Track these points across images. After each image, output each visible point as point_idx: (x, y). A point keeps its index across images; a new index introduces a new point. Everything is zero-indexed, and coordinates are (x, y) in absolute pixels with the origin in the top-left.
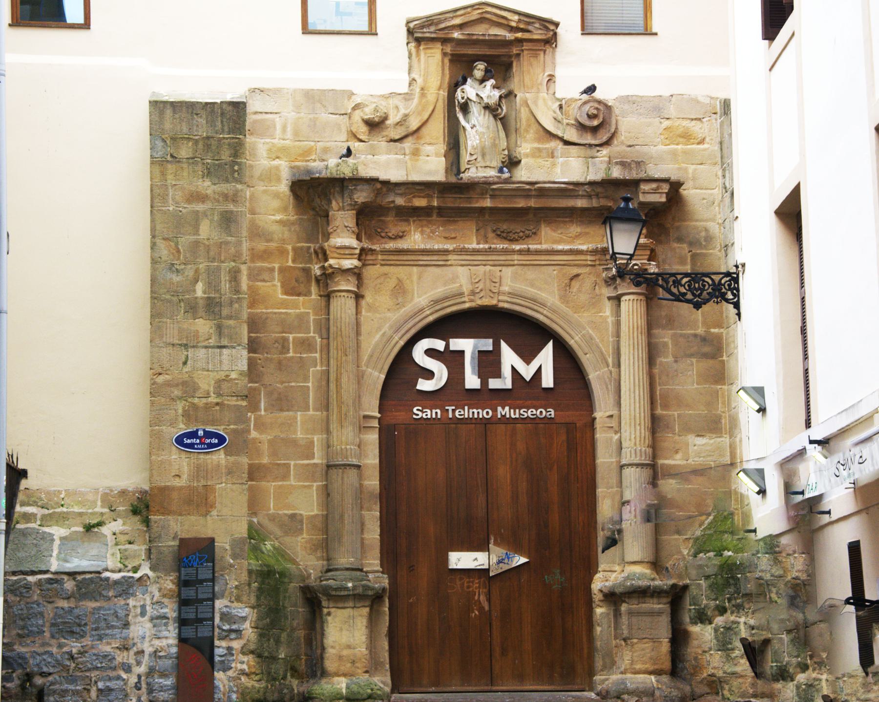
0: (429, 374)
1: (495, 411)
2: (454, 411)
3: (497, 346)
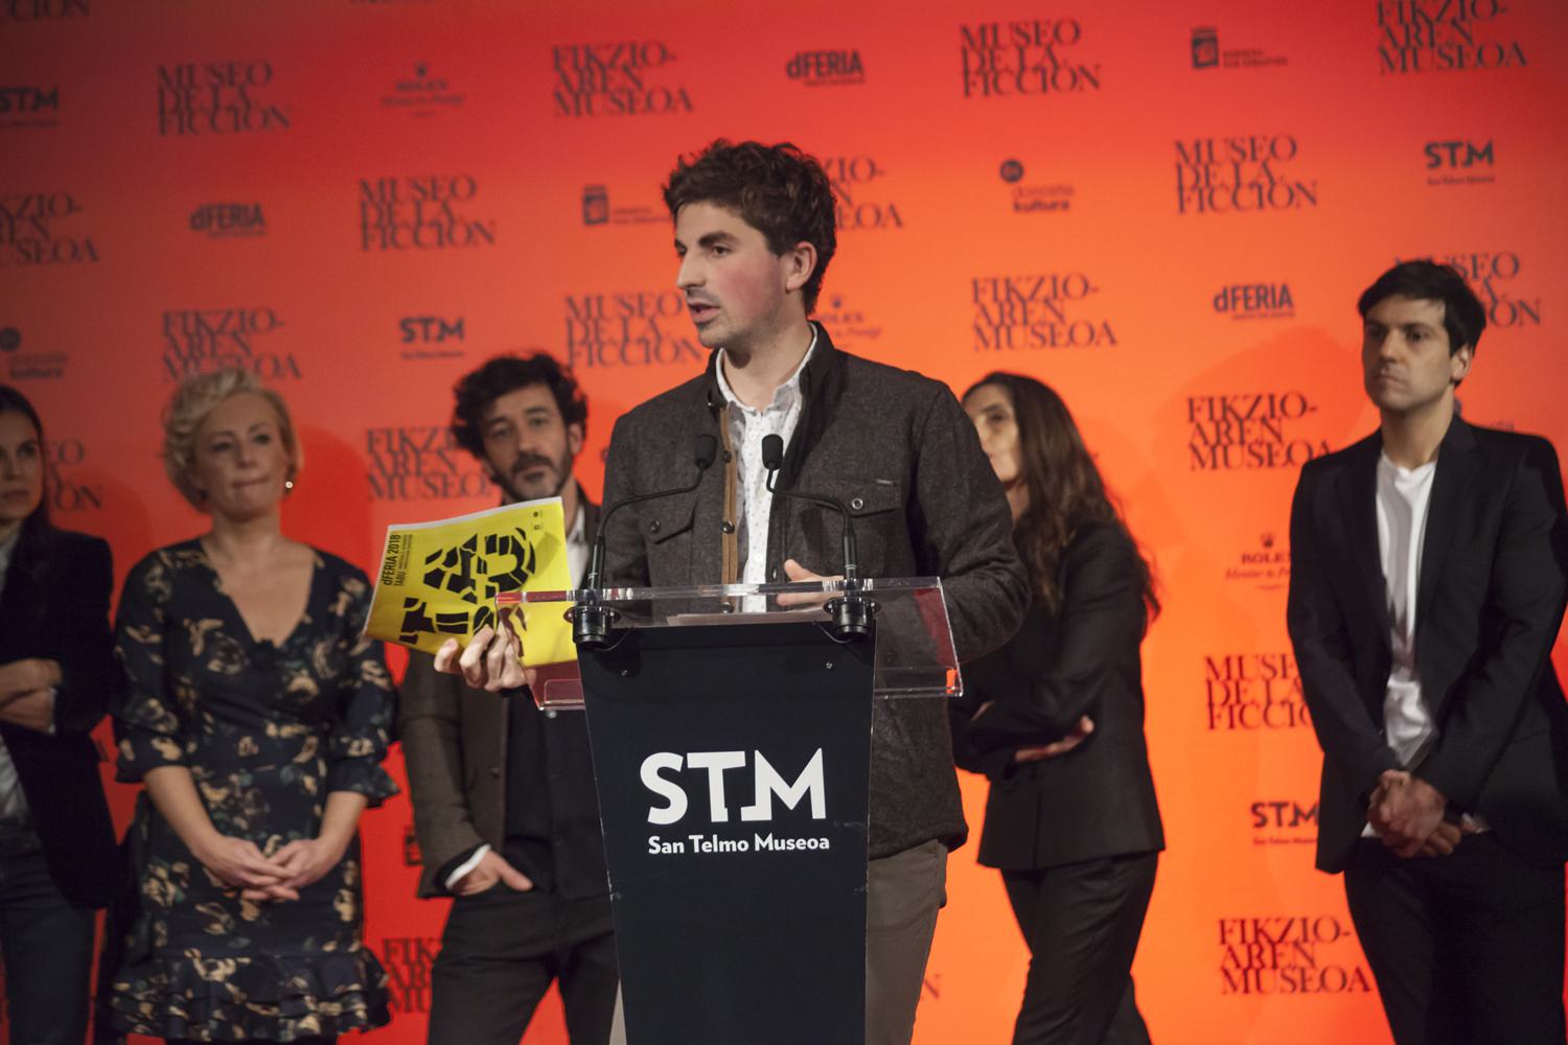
1: (752, 844)
2: (701, 842)
3: (750, 760)
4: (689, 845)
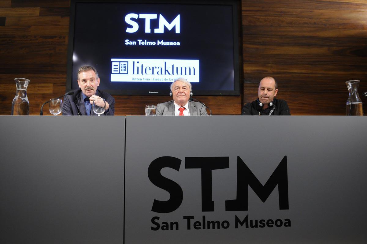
0: (131, 27)
1: (157, 43)
2: (141, 42)
3: (158, 17)
4: (138, 43)
